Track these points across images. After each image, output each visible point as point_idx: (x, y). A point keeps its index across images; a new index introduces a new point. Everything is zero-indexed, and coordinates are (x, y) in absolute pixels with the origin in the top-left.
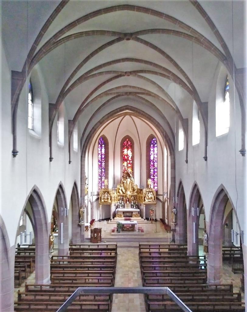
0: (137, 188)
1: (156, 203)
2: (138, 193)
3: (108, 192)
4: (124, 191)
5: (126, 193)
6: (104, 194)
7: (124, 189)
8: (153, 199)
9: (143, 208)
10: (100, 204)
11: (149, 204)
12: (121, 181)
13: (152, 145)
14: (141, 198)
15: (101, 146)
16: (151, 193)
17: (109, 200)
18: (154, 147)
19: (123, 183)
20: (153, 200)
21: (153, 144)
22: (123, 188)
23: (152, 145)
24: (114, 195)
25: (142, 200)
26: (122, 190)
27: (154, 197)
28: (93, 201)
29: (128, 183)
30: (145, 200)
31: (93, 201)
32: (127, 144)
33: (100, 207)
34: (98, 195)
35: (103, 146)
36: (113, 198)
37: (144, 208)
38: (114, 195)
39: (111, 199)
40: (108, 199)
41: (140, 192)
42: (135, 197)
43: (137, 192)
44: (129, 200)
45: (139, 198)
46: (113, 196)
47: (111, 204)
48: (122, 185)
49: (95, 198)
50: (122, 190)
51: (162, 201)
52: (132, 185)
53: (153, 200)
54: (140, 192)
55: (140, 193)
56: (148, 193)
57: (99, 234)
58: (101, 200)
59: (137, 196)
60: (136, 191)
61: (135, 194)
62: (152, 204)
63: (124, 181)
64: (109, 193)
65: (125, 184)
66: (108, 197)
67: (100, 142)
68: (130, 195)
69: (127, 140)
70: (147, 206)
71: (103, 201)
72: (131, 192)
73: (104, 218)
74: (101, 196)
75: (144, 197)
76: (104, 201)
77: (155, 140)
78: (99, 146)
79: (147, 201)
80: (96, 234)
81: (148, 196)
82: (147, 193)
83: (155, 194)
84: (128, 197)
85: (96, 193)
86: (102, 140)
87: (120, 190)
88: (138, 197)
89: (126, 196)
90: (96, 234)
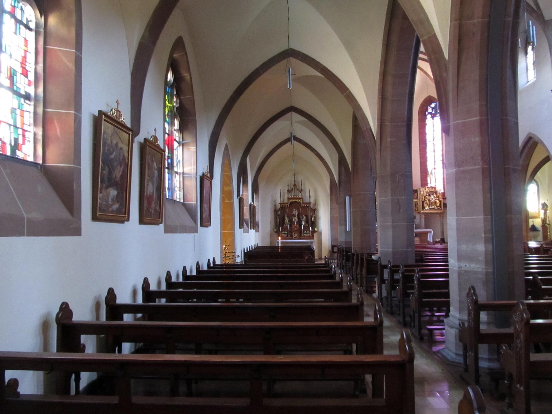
8: (438, 205)
11: (431, 213)
16: (435, 196)
20: (437, 207)
21: (430, 113)
27: (440, 201)
30: (423, 207)
37: (423, 220)
56: (429, 195)
62: (437, 213)
70: (428, 216)
75: (423, 202)
79: (427, 208)
81: (429, 200)
83: (440, 197)
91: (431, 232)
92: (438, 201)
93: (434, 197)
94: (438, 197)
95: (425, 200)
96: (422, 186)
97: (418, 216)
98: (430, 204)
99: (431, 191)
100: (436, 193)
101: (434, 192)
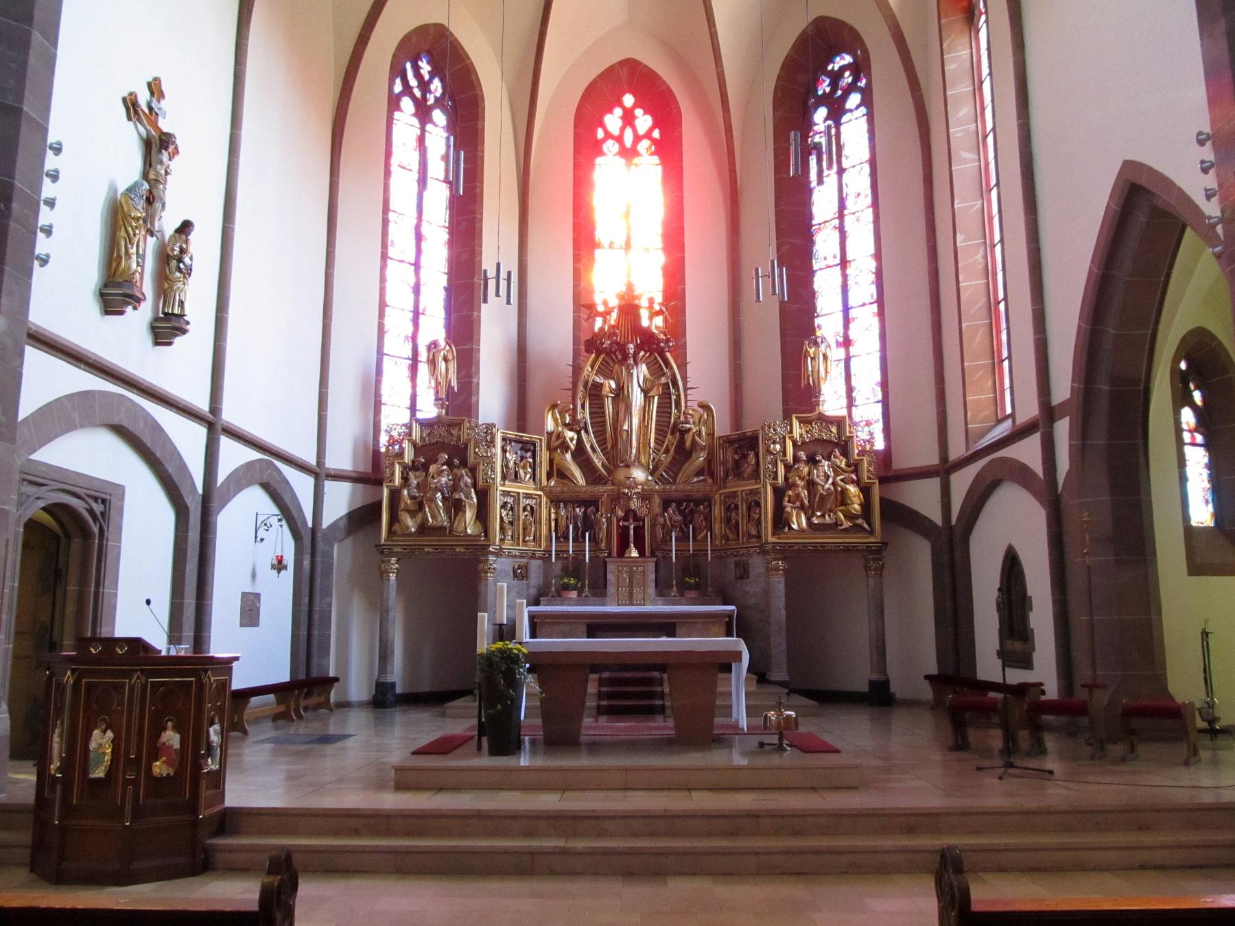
0: (711, 435)
1: (885, 544)
2: (720, 472)
3: (459, 455)
4: (598, 460)
5: (621, 474)
6: (425, 467)
7: (602, 443)
9: (770, 585)
10: (383, 551)
11: (820, 550)
12: (575, 384)
13: (821, 114)
14: (749, 508)
15: (423, 113)
17: (470, 515)
18: (837, 112)
19: (595, 392)
20: (850, 516)
22: (589, 440)
23: (821, 114)
24: (515, 488)
25: (759, 522)
26: (580, 454)
27: (865, 490)
28: (327, 520)
29: (637, 398)
30: (781, 520)
31: (327, 520)
32: (622, 129)
33: (383, 575)
34: (371, 474)
35: (439, 116)
36: (497, 513)
38: (511, 487)
39: (483, 515)
40: (455, 507)
41: (737, 464)
42: (691, 508)
43: (708, 470)
44: (639, 531)
45: (728, 520)
46: (500, 489)
47: (482, 550)
48: (584, 415)
49: (339, 501)
50: (580, 454)
51: (937, 518)
52: (664, 409)
53: (850, 516)
54: (737, 464)
55: (738, 474)
56: (812, 461)
57: (171, 738)
58: (394, 518)
59: (707, 500)
60: (701, 458)
61: (689, 481)
62: (848, 549)
63: (599, 380)
64: (464, 463)
65: (609, 405)
66: (455, 487)
67: (413, 82)
68: (645, 496)
69: (629, 100)
70: (803, 563)
71: (411, 524)
72: (656, 468)
73: (425, 687)
74: (397, 481)
75: (779, 493)
76: (423, 529)
77: (843, 69)
78: (407, 104)
79: (799, 521)
80: (101, 741)
81: (811, 485)
82: (803, 455)
84: (634, 504)
85: (341, 457)
86: (432, 75)
87: (567, 448)
88: (717, 511)
89: (618, 498)
90: (101, 741)
91: (737, 656)
92: (852, 489)
93: (837, 470)
94: (856, 471)
95: (789, 485)
96: (787, 416)
97: (757, 565)
98: (816, 501)
99: (820, 441)
100: (844, 446)
101: (835, 440)
